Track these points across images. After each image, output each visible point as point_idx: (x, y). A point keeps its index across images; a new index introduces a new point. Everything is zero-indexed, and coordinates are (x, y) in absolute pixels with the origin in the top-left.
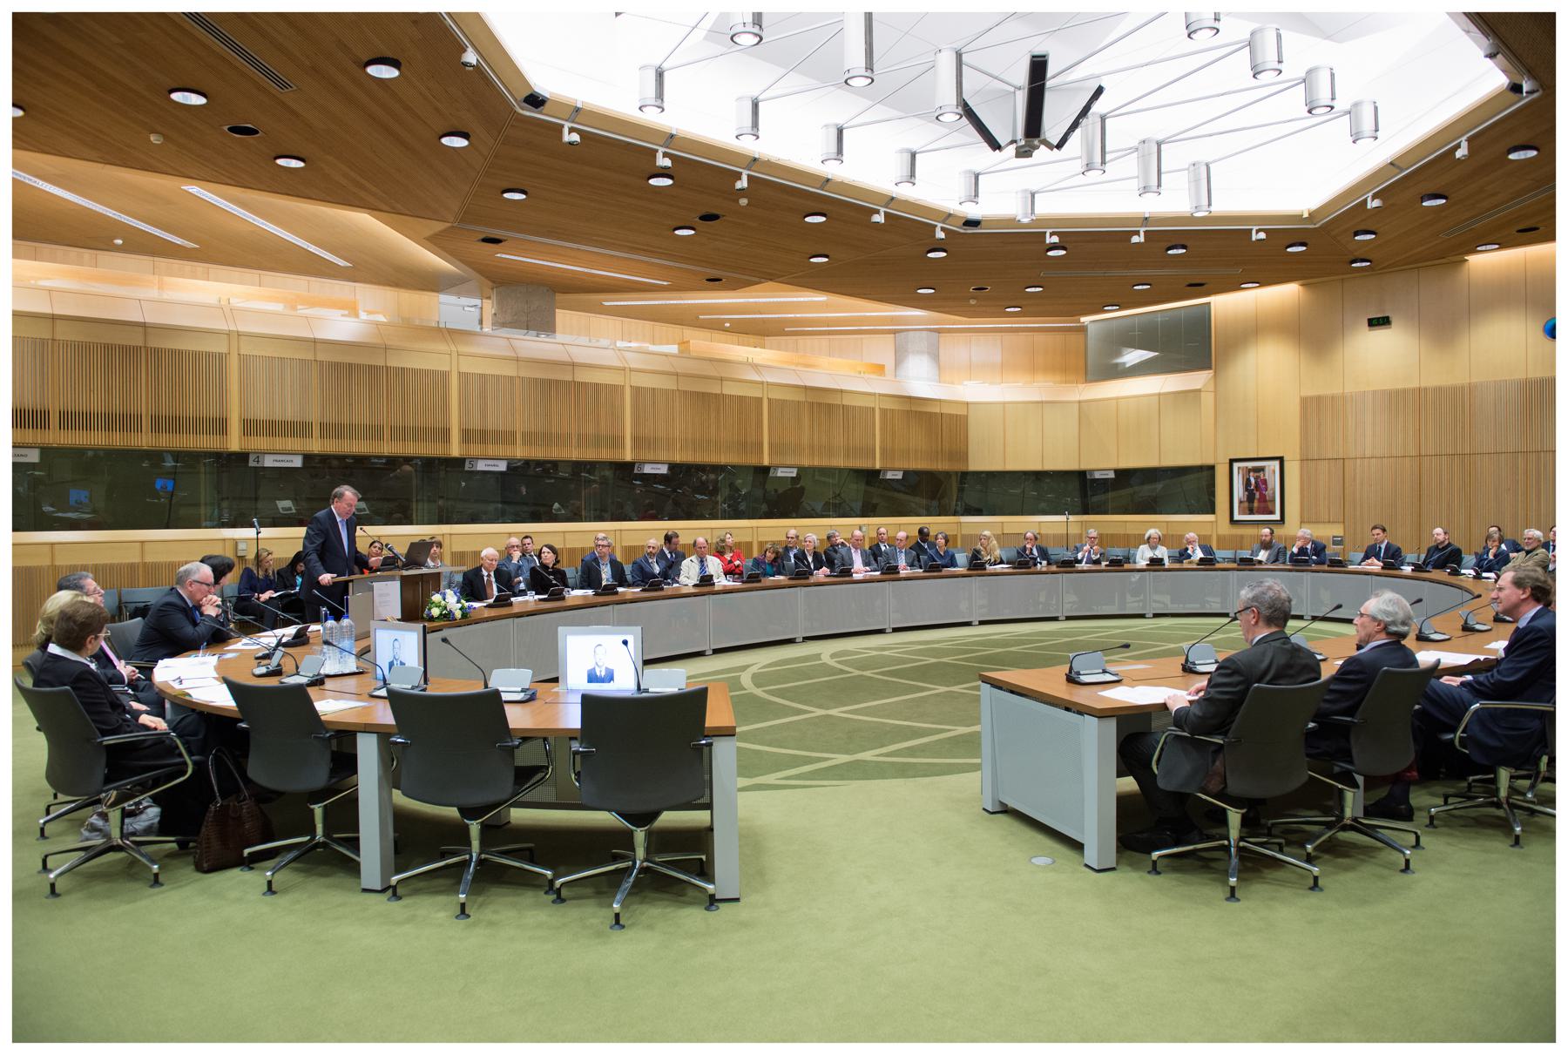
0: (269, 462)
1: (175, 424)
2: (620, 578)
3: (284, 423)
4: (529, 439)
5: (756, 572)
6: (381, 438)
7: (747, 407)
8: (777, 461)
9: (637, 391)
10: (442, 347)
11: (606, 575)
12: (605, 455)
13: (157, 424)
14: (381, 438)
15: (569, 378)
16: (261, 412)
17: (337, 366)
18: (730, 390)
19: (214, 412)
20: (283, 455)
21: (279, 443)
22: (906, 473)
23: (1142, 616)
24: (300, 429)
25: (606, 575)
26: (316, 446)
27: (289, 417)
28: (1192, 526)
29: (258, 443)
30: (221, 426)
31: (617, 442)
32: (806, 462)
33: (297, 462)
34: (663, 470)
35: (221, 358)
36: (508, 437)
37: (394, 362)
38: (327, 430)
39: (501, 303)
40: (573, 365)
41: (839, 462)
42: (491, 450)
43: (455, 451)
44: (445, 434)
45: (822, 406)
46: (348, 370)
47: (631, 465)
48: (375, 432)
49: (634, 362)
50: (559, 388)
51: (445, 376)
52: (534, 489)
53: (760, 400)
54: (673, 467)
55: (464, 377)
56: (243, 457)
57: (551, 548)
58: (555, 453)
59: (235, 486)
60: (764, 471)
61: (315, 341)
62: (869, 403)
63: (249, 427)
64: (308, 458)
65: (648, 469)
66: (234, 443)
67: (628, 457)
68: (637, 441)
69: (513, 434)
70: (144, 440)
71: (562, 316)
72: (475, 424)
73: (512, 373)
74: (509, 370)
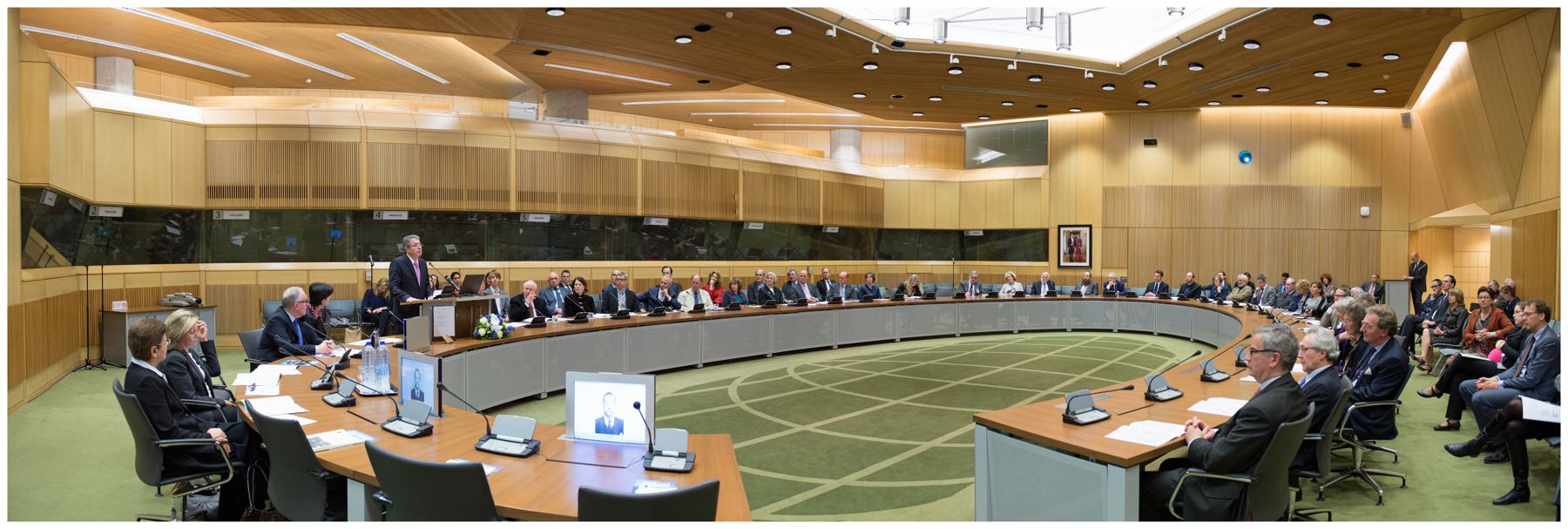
0: (386, 216)
2: (633, 304)
3: (395, 189)
4: (567, 198)
5: (729, 298)
7: (728, 178)
8: (749, 218)
9: (646, 163)
10: (505, 132)
11: (622, 300)
12: (622, 211)
15: (596, 153)
16: (381, 182)
17: (431, 148)
18: (714, 164)
19: (351, 183)
20: (394, 211)
22: (841, 228)
23: (1011, 332)
24: (406, 193)
25: (622, 300)
26: (417, 205)
27: (399, 184)
28: (1044, 270)
29: (380, 203)
30: (355, 192)
31: (631, 200)
32: (770, 219)
33: (405, 216)
34: (665, 223)
35: (356, 145)
36: (552, 197)
37: (469, 144)
38: (426, 193)
39: (549, 105)
40: (599, 143)
41: (795, 220)
42: (539, 207)
43: (513, 208)
44: (505, 196)
45: (782, 177)
46: (440, 151)
47: (641, 219)
48: (457, 194)
49: (645, 141)
50: (588, 160)
51: (506, 152)
52: (569, 236)
53: (736, 172)
54: (672, 221)
55: (520, 153)
56: (369, 213)
57: (582, 280)
58: (585, 209)
59: (363, 233)
60: (739, 225)
61: (416, 131)
62: (815, 177)
63: (374, 192)
64: (412, 213)
65: (654, 222)
66: (364, 204)
67: (639, 213)
68: (645, 200)
69: (555, 195)
70: (309, 203)
71: (591, 112)
72: (527, 188)
73: (554, 149)
74: (553, 148)
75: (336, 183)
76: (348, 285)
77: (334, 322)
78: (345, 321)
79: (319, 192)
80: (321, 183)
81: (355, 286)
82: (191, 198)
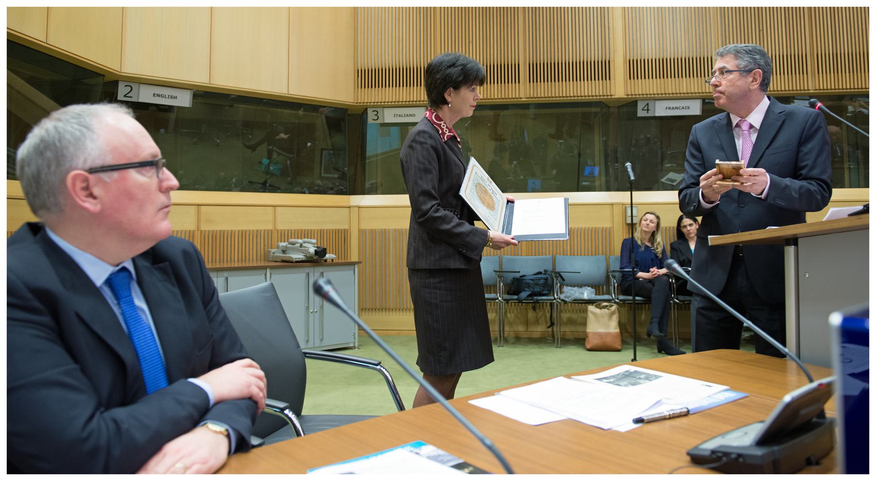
0: (661, 110)
1: (551, 71)
6: (803, 71)
13: (537, 73)
14: (803, 71)
16: (650, 50)
19: (594, 54)
21: (671, 85)
30: (603, 70)
66: (619, 88)
75: (569, 56)
76: (595, 231)
77: (571, 293)
78: (587, 293)
79: (537, 73)
80: (543, 57)
81: (607, 233)
82: (331, 87)
